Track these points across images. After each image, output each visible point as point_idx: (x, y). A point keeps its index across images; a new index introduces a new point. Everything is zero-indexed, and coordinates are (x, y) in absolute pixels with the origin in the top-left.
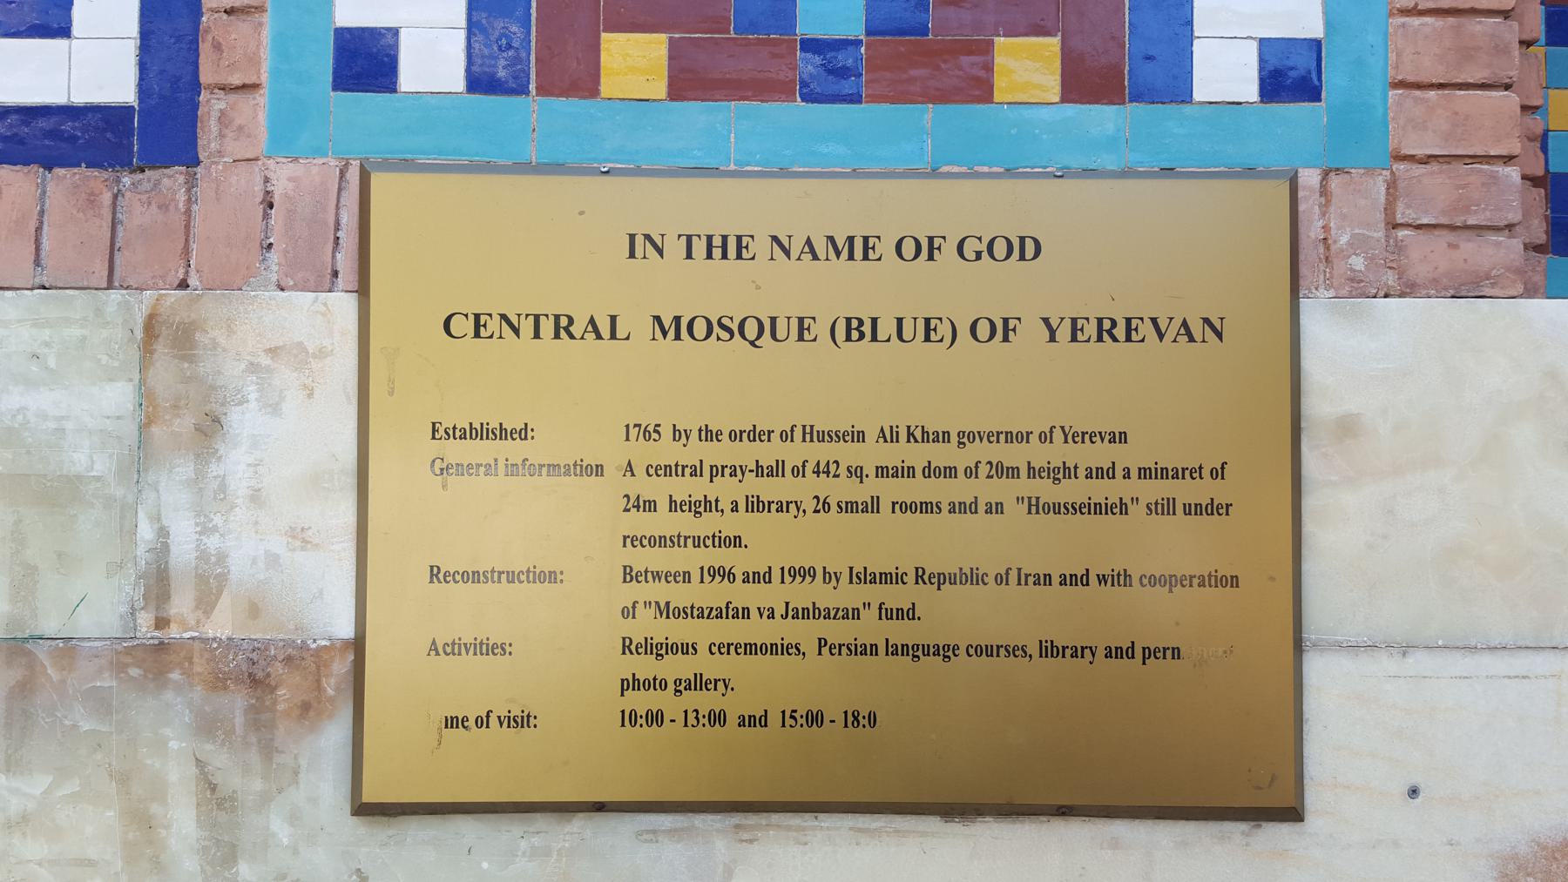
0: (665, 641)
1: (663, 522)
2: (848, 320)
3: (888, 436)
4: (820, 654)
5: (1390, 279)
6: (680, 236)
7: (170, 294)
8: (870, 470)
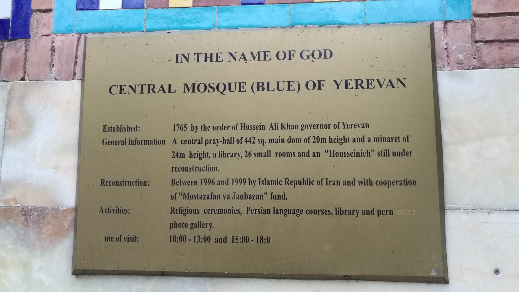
0: (187, 208)
1: (189, 162)
2: (258, 83)
3: (274, 127)
4: (247, 213)
5: (475, 62)
6: (195, 54)
7: (18, 83)
8: (267, 140)
